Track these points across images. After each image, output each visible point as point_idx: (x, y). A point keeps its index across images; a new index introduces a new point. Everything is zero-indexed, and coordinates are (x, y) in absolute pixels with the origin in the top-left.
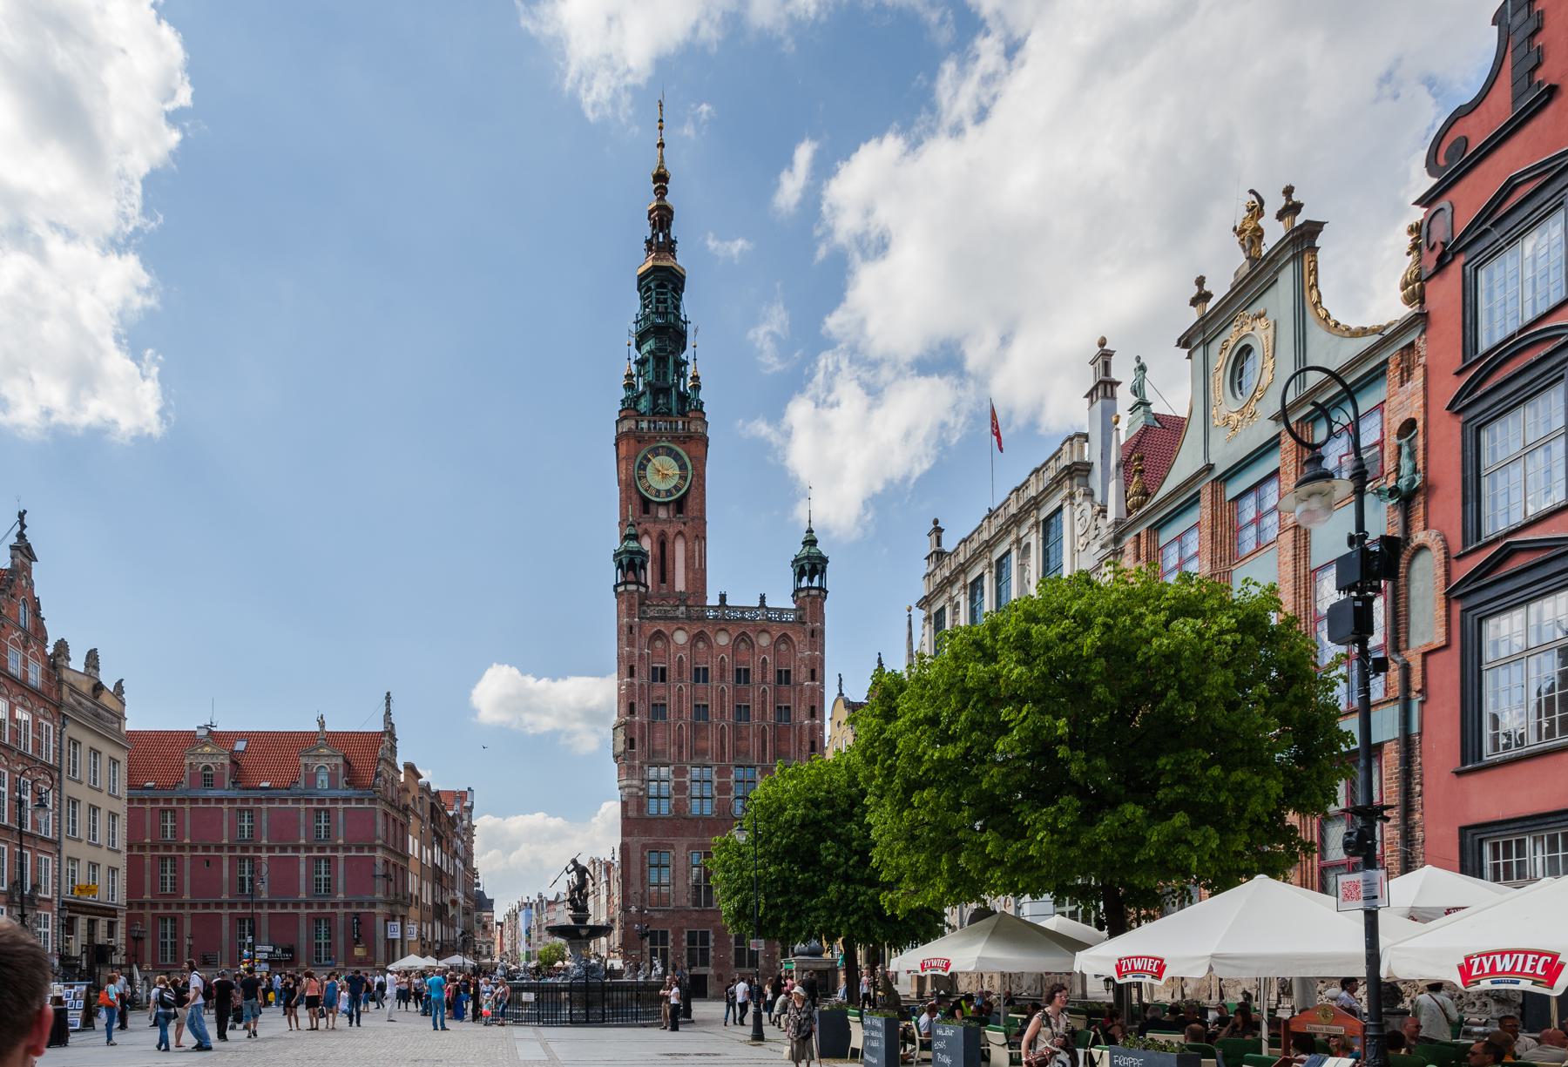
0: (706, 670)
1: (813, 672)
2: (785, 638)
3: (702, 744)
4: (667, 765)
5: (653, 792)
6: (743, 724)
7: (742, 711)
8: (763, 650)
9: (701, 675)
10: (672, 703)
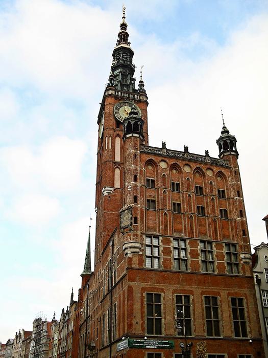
0: (178, 185)
1: (238, 192)
2: (220, 174)
3: (179, 226)
4: (157, 237)
5: (148, 253)
6: (201, 217)
7: (201, 210)
8: (210, 178)
9: (176, 187)
10: (159, 200)
